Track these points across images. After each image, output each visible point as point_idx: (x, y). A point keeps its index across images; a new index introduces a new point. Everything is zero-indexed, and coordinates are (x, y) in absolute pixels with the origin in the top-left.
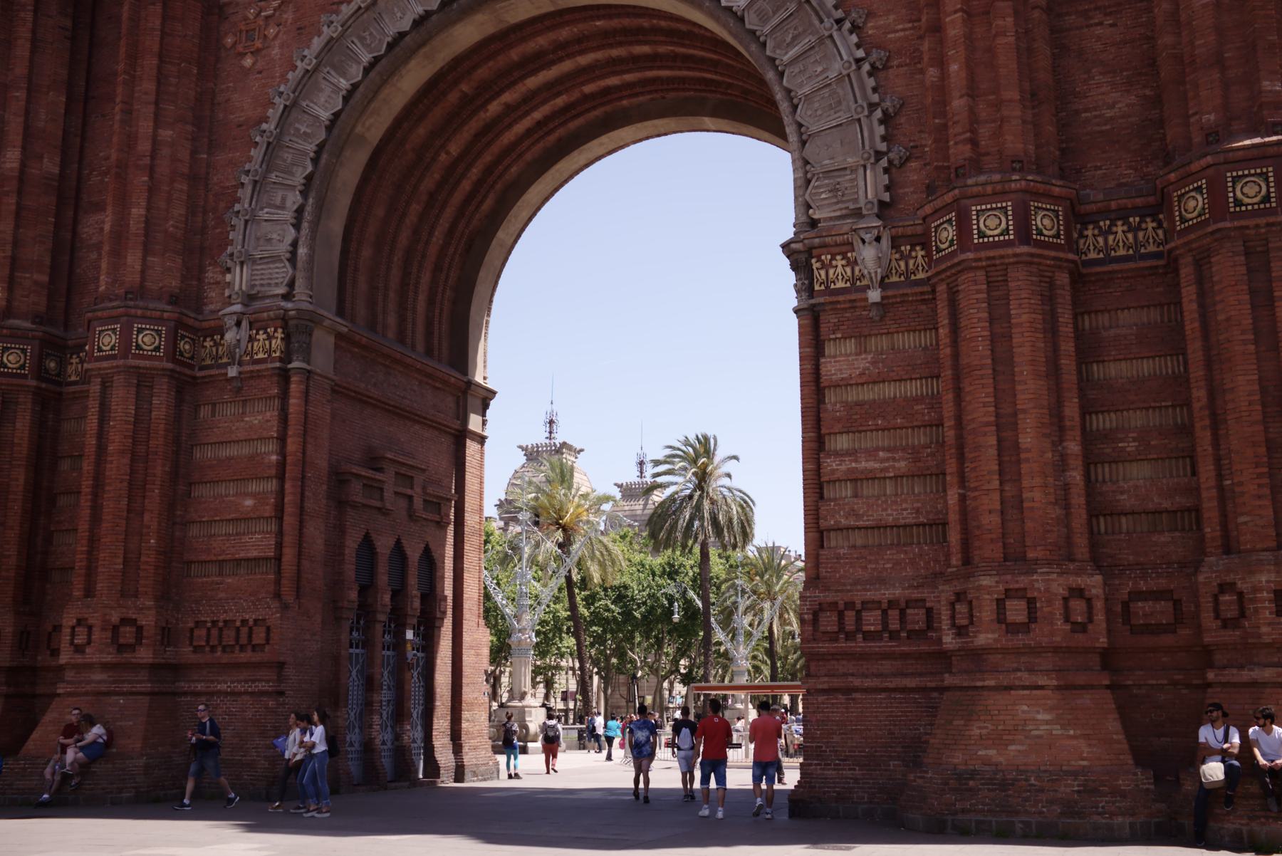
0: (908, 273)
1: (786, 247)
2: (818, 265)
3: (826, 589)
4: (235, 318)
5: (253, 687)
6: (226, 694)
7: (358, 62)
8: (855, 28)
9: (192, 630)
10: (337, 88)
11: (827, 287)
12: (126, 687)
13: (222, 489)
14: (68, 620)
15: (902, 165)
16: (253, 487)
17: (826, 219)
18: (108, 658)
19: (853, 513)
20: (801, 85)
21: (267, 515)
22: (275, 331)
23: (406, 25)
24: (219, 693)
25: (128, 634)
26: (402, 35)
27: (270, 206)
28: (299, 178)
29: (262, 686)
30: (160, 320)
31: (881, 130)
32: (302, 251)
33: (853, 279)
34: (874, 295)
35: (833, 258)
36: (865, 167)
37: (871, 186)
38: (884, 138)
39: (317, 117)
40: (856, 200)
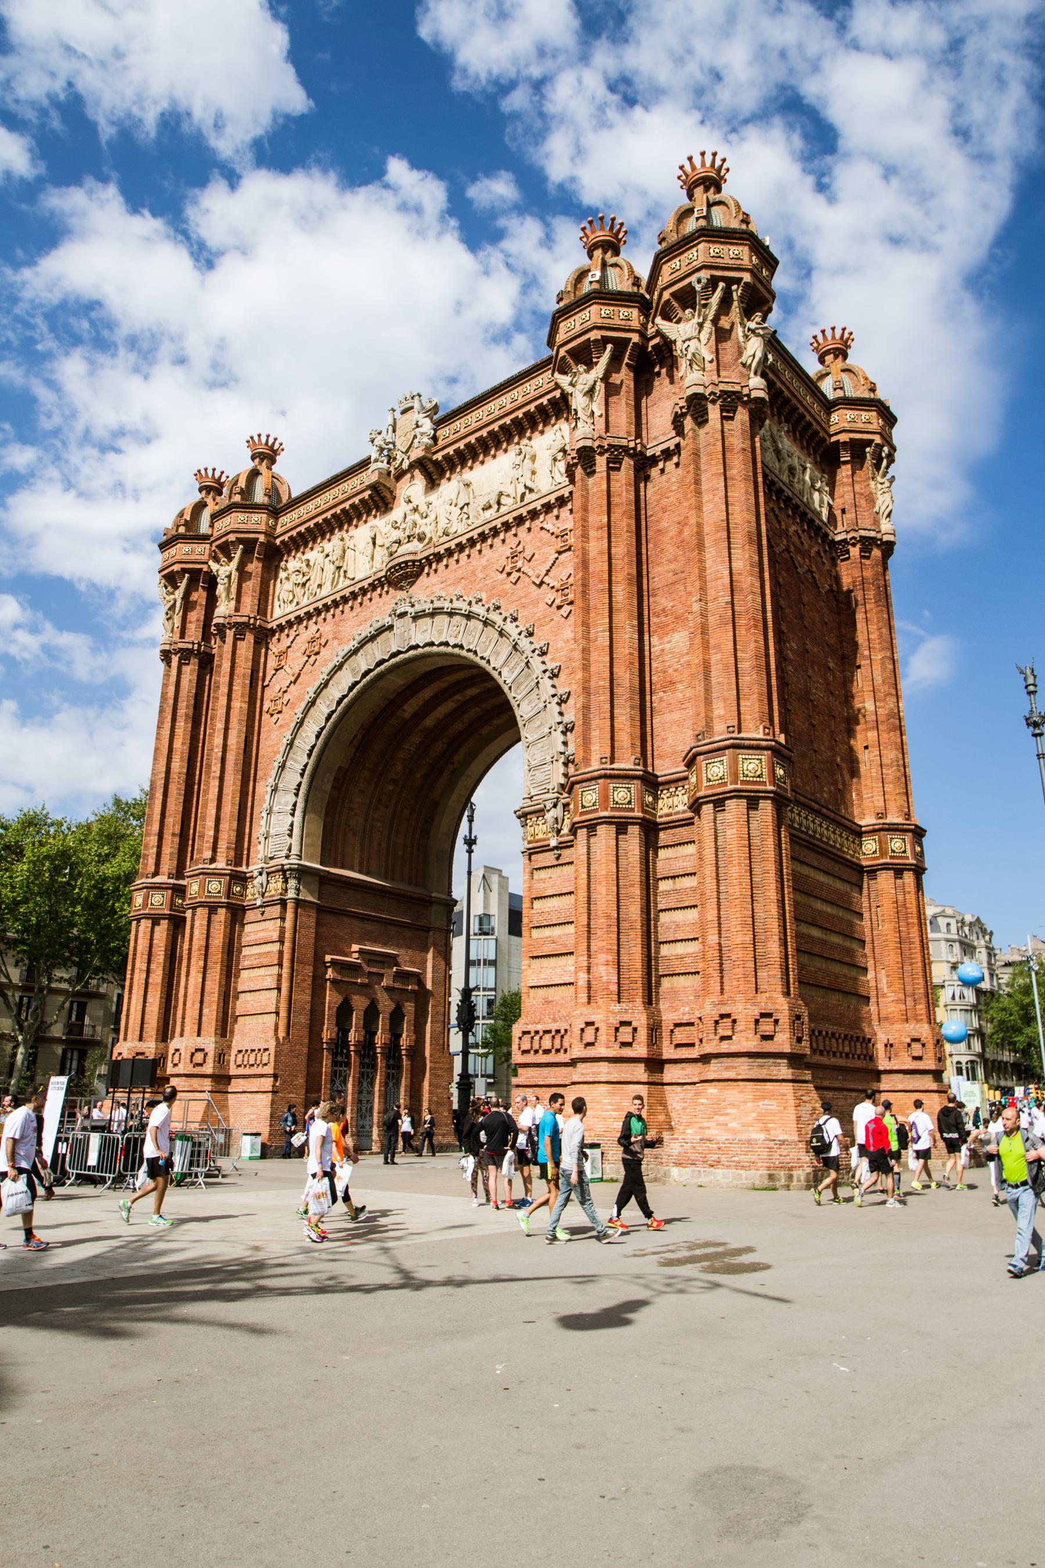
34: (553, 843)
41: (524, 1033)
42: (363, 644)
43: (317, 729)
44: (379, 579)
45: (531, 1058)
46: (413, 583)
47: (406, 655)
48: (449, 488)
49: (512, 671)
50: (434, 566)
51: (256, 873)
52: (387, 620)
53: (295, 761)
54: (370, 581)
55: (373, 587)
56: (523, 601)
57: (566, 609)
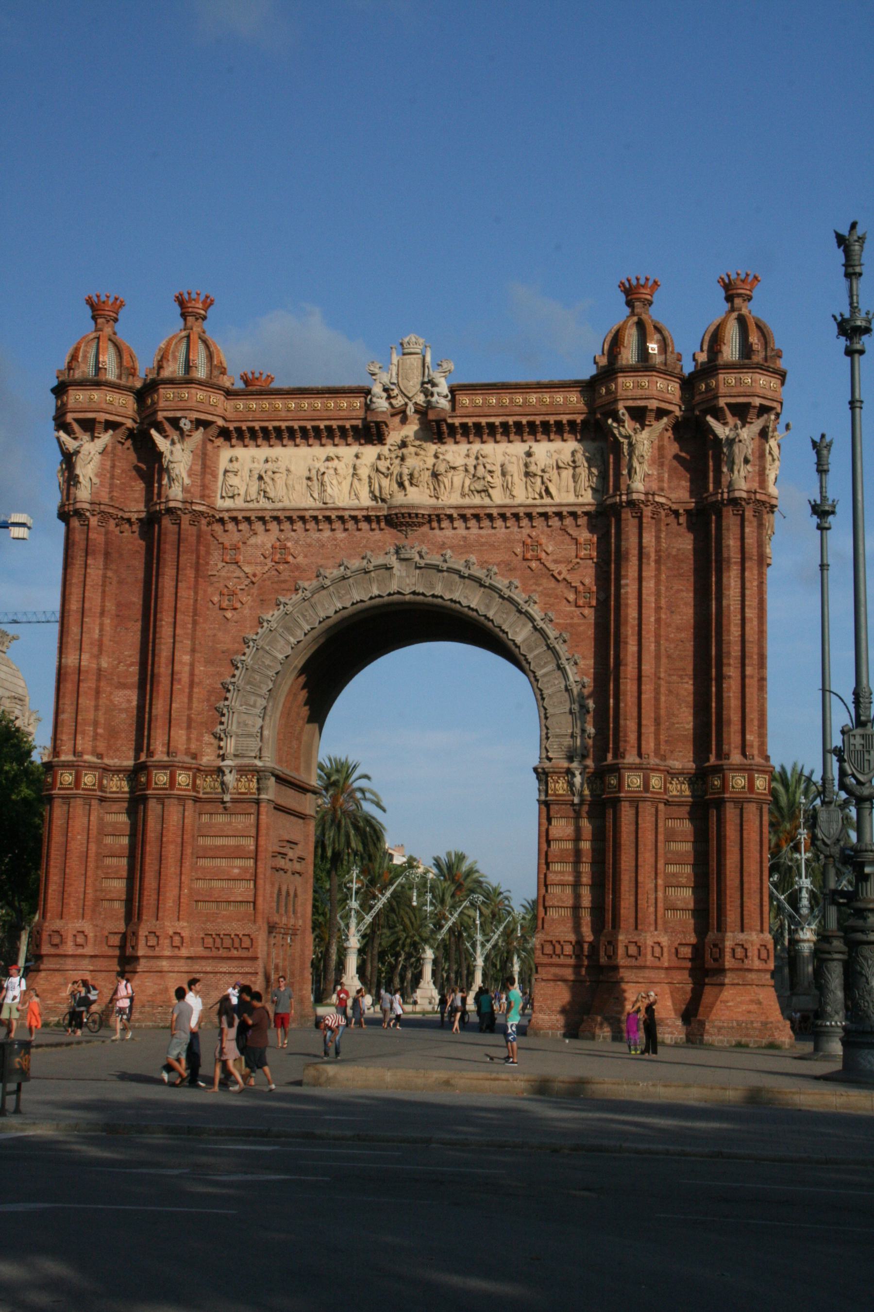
1: (535, 770)
3: (547, 934)
4: (230, 769)
5: (242, 970)
6: (225, 973)
7: (302, 629)
9: (203, 938)
10: (288, 642)
12: (176, 969)
13: (218, 862)
14: (143, 932)
16: (238, 862)
18: (167, 953)
19: (561, 900)
20: (548, 688)
21: (248, 878)
22: (253, 776)
23: (331, 612)
24: (221, 973)
25: (177, 939)
26: (328, 617)
27: (247, 704)
28: (264, 690)
29: (247, 970)
30: (189, 769)
32: (266, 733)
35: (559, 778)
39: (275, 658)
44: (378, 517)
45: (555, 960)
47: (407, 598)
48: (456, 452)
54: (365, 513)
55: (368, 519)
57: (586, 611)
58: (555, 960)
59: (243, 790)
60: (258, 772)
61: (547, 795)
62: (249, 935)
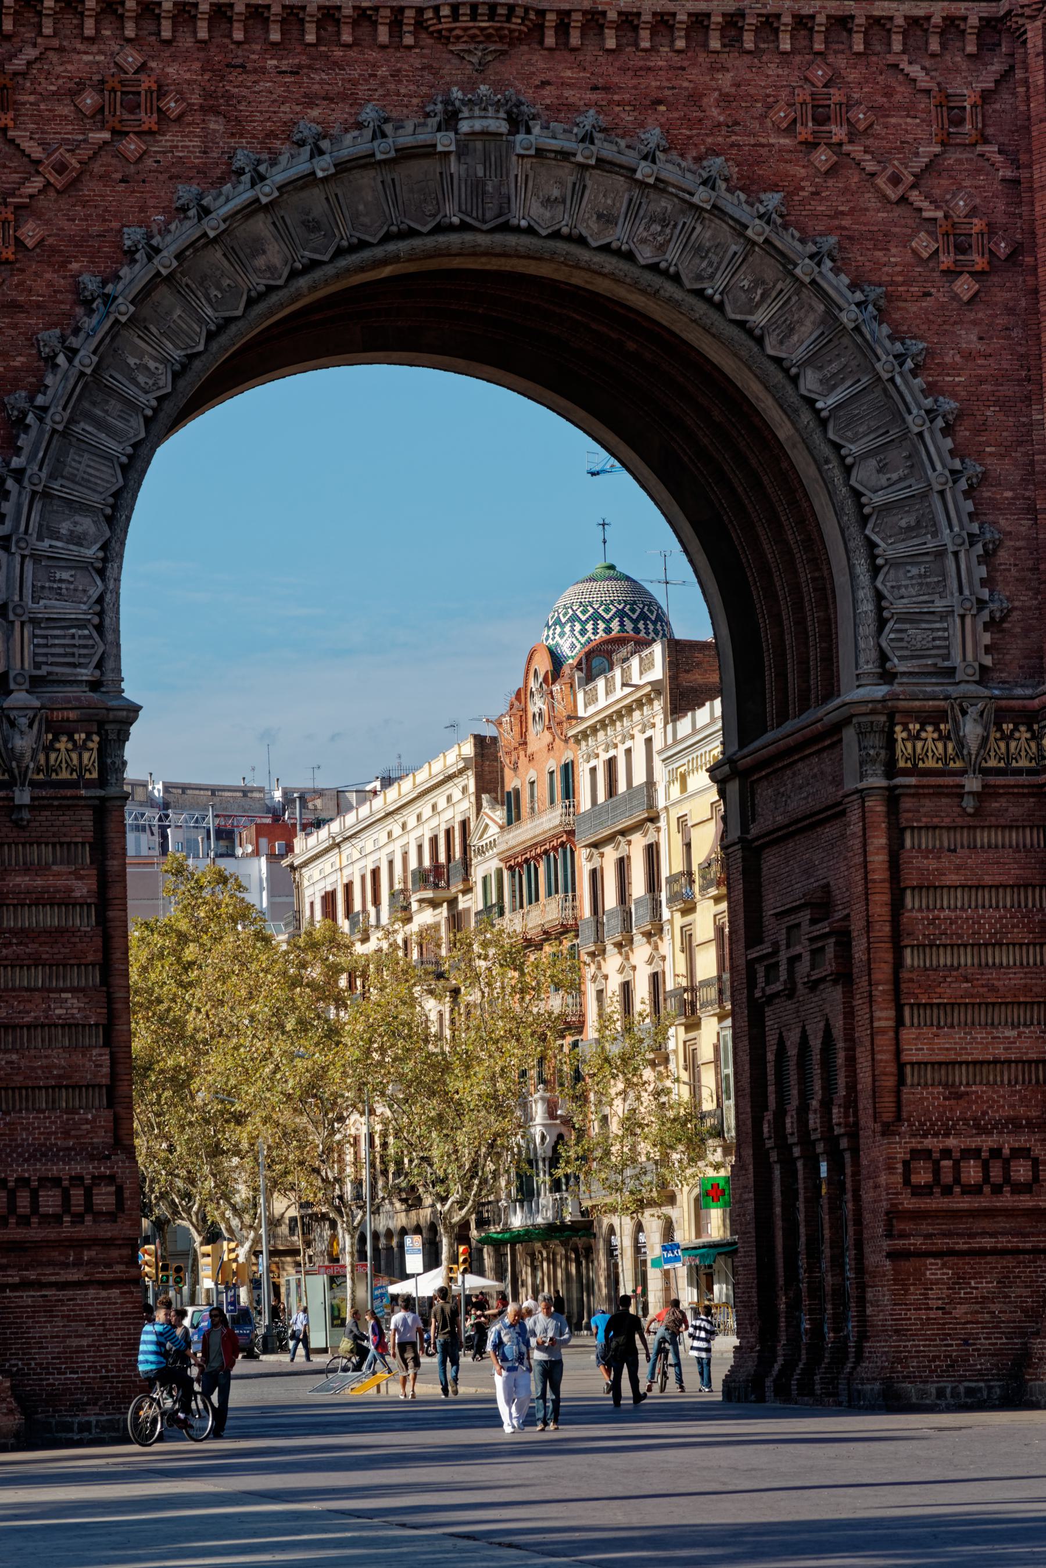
0: (1008, 757)
2: (904, 735)
8: (948, 430)
11: (915, 765)
15: (1003, 619)
17: (904, 673)
22: (89, 738)
31: (983, 571)
33: (945, 758)
34: (973, 783)
36: (963, 617)
37: (967, 646)
38: (984, 582)
40: (947, 657)
41: (917, 1154)
42: (343, 168)
43: (178, 354)
45: (937, 1202)
46: (503, 53)
47: (483, 240)
49: (829, 385)
50: (575, 40)
51: (23, 722)
52: (445, 141)
53: (101, 425)
56: (846, 222)
57: (965, 287)
58: (937, 1202)
59: (65, 775)
60: (101, 724)
61: (891, 770)
62: (111, 1179)
